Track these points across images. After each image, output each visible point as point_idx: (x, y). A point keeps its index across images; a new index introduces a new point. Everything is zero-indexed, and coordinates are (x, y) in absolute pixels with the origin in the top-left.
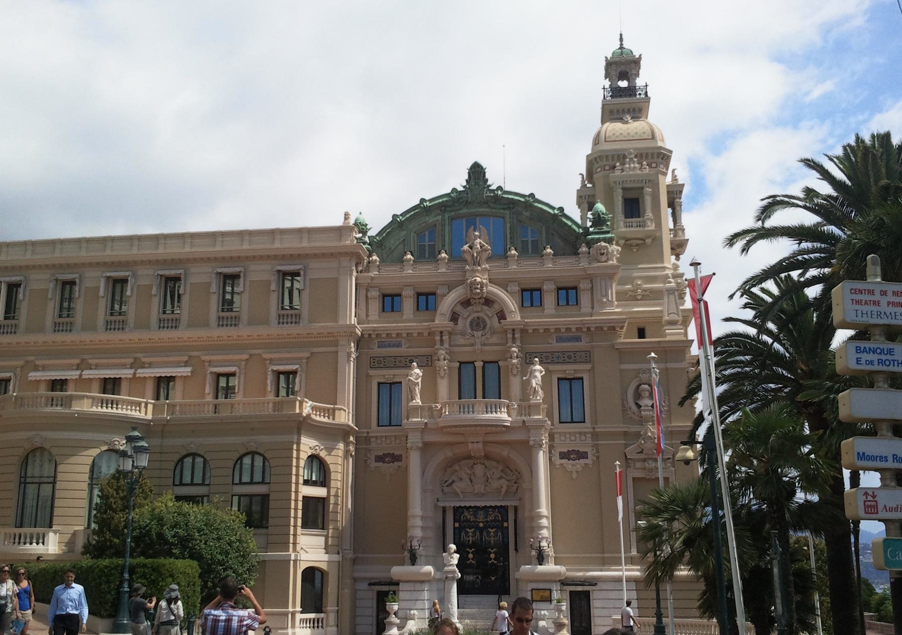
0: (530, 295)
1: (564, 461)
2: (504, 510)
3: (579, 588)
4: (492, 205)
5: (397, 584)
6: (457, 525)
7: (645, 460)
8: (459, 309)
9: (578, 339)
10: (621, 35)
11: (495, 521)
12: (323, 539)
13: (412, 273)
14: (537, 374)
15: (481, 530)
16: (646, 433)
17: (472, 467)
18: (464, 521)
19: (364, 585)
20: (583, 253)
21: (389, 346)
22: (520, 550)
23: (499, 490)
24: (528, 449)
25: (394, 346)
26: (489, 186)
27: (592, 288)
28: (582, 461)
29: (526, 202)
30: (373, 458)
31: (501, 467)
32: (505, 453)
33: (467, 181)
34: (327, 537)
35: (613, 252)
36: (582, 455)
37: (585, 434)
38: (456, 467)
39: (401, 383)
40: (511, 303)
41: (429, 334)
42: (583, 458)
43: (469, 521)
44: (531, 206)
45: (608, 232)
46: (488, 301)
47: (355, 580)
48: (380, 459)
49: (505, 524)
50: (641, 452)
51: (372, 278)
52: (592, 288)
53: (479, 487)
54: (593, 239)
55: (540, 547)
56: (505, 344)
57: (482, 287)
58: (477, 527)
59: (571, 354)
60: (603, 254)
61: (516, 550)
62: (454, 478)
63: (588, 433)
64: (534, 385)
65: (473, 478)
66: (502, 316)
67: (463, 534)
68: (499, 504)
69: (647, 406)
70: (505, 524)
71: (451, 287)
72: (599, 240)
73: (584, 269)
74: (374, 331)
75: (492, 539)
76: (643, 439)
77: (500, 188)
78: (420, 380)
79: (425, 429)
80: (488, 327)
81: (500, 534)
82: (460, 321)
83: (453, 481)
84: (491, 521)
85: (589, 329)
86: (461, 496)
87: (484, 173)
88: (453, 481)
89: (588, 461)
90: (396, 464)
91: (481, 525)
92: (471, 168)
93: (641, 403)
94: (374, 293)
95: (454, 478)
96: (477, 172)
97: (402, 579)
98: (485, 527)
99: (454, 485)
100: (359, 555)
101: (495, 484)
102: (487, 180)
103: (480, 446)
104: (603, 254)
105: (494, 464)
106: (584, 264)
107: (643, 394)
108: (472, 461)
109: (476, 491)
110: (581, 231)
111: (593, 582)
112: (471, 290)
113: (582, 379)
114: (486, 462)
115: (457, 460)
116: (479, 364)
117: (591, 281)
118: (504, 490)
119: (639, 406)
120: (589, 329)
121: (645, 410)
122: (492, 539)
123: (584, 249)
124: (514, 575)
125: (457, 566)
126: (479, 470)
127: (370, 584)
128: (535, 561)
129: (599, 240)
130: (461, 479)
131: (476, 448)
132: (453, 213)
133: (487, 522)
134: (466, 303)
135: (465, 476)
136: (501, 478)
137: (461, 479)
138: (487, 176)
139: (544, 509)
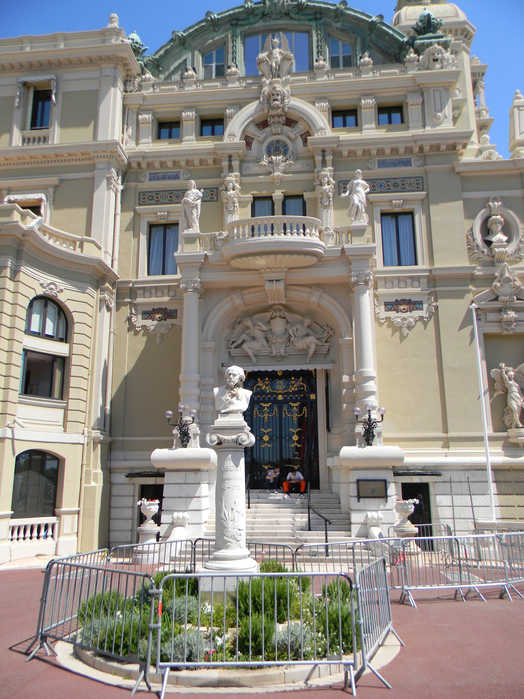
0: (344, 115)
1: (392, 314)
2: (308, 376)
3: (416, 480)
4: (293, 15)
5: (160, 474)
7: (500, 310)
8: (253, 130)
9: (407, 163)
13: (195, 87)
14: (360, 189)
15: (280, 404)
16: (502, 275)
17: (269, 322)
20: (411, 61)
21: (164, 178)
22: (333, 430)
23: (304, 352)
24: (346, 292)
25: (170, 178)
27: (423, 102)
28: (416, 314)
29: (337, 9)
31: (307, 321)
32: (315, 298)
35: (448, 60)
36: (413, 304)
37: (418, 278)
39: (178, 224)
40: (319, 117)
41: (215, 161)
42: (417, 309)
44: (343, 14)
45: (441, 37)
49: (312, 397)
50: (496, 299)
51: (144, 98)
52: (423, 102)
53: (279, 349)
54: (423, 44)
55: (370, 419)
56: (313, 172)
57: (283, 100)
58: (275, 401)
60: (435, 60)
61: (328, 429)
62: (244, 337)
63: (423, 277)
64: (356, 202)
65: (270, 336)
68: (305, 367)
69: (500, 241)
70: (312, 397)
72: (431, 44)
73: (414, 79)
74: (144, 158)
76: (499, 281)
79: (204, 264)
80: (290, 152)
82: (254, 145)
83: (243, 342)
84: (294, 393)
85: (421, 149)
86: (254, 359)
88: (243, 342)
90: (170, 321)
91: (280, 398)
93: (494, 239)
94: (147, 117)
95: (244, 337)
97: (168, 467)
98: (285, 401)
99: (245, 346)
101: (300, 344)
103: (281, 286)
104: (435, 60)
105: (298, 317)
106: (412, 72)
107: (493, 228)
108: (268, 315)
109: (274, 353)
110: (405, 39)
111: (434, 471)
112: (269, 104)
114: (287, 315)
115: (249, 314)
117: (422, 94)
118: (311, 351)
120: (421, 149)
121: (498, 247)
122: (295, 415)
124: (325, 462)
125: (248, 415)
127: (130, 476)
129: (431, 44)
130: (254, 338)
131: (275, 292)
132: (246, 27)
133: (288, 393)
135: (258, 334)
136: (308, 335)
137: (254, 338)
139: (370, 368)
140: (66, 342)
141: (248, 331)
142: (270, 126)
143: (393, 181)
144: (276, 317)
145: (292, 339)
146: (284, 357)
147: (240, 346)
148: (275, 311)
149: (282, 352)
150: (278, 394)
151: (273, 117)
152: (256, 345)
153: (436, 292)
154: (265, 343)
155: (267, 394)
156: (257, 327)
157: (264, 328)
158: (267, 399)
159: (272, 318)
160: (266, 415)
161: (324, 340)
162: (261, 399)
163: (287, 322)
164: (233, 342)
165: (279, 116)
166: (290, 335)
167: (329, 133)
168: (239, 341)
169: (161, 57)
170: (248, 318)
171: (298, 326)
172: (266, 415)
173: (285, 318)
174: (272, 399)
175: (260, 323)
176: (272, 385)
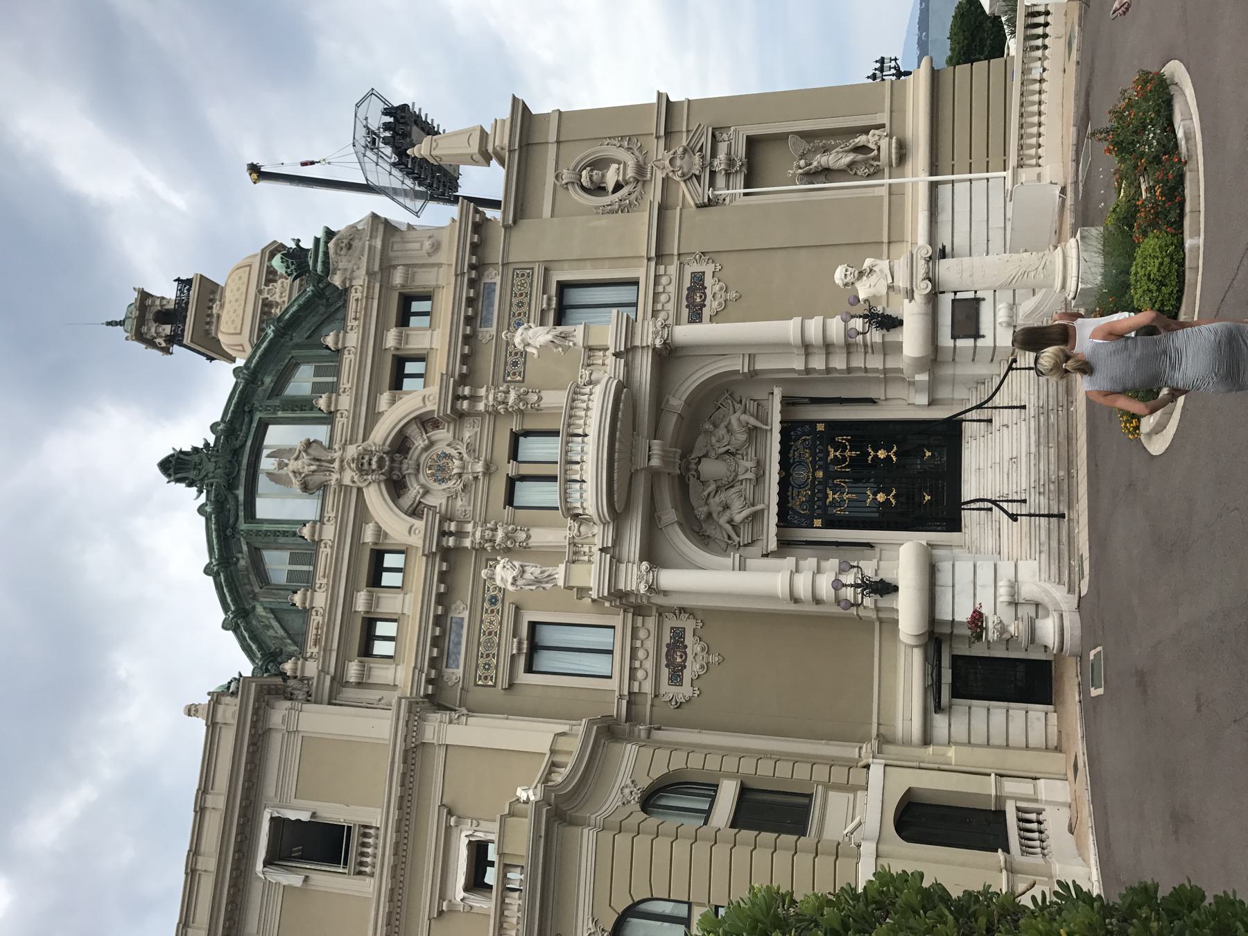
1: (706, 312)
6: (818, 522)
10: (109, 324)
11: (812, 449)
12: (832, 795)
15: (829, 476)
18: (812, 509)
19: (940, 721)
26: (207, 445)
28: (708, 281)
30: (674, 689)
33: (190, 485)
34: (829, 786)
38: (701, 511)
42: (702, 280)
43: (811, 500)
46: (401, 444)
47: (927, 740)
48: (676, 678)
58: (824, 483)
59: (515, 301)
62: (723, 520)
66: (426, 422)
67: (837, 511)
68: (776, 437)
70: (820, 427)
71: (362, 514)
74: (421, 671)
75: (848, 453)
77: (213, 428)
78: (517, 564)
80: (449, 451)
81: (839, 439)
83: (730, 522)
84: (813, 455)
86: (759, 507)
87: (181, 452)
88: (730, 522)
89: (708, 269)
91: (820, 474)
92: (169, 476)
96: (177, 467)
99: (738, 518)
100: (874, 732)
102: (195, 449)
103: (656, 444)
105: (701, 441)
108: (693, 482)
109: (750, 475)
113: (563, 286)
116: (511, 469)
118: (753, 421)
119: (618, 186)
123: (337, 280)
126: (711, 468)
128: (892, 336)
132: (241, 514)
133: (814, 463)
134: (396, 487)
137: (727, 507)
138: (188, 448)
140: (717, 786)
141: (715, 515)
142: (404, 477)
143: (514, 309)
144: (697, 470)
145: (732, 450)
146: (758, 462)
147: (735, 528)
148: (688, 469)
149: (749, 464)
150: (814, 478)
151: (391, 469)
152: (737, 504)
153: (679, 255)
154: (733, 490)
155: (814, 494)
156: (711, 501)
157: (712, 487)
158: (820, 495)
159: (698, 478)
160: (845, 496)
161: (737, 406)
162: (820, 503)
163: (706, 456)
164: (729, 538)
165: (392, 460)
166: (727, 452)
167: (434, 389)
168: (729, 527)
169: (260, 648)
170: (696, 512)
171: (714, 440)
172: (845, 496)
173: (700, 459)
174: (820, 487)
175: (706, 493)
176: (800, 487)
